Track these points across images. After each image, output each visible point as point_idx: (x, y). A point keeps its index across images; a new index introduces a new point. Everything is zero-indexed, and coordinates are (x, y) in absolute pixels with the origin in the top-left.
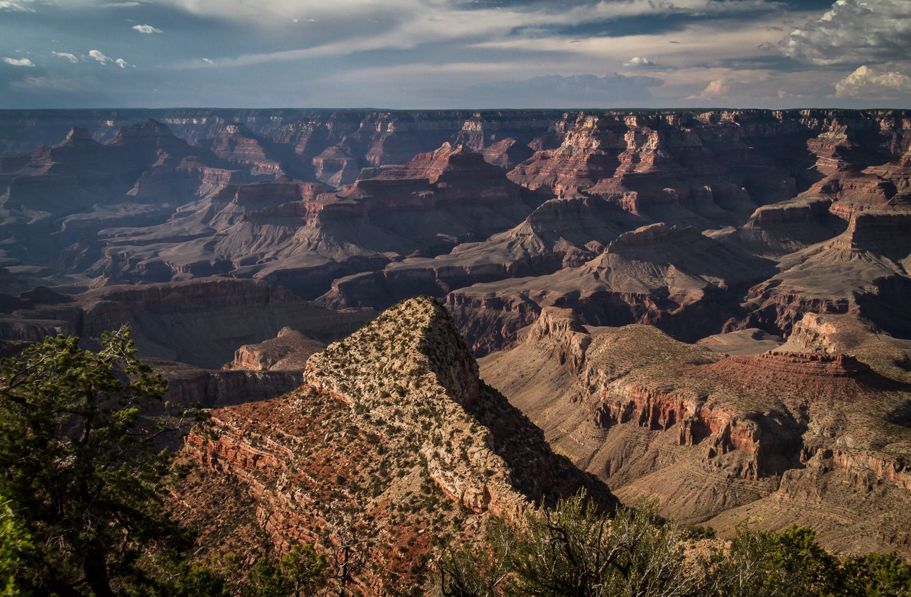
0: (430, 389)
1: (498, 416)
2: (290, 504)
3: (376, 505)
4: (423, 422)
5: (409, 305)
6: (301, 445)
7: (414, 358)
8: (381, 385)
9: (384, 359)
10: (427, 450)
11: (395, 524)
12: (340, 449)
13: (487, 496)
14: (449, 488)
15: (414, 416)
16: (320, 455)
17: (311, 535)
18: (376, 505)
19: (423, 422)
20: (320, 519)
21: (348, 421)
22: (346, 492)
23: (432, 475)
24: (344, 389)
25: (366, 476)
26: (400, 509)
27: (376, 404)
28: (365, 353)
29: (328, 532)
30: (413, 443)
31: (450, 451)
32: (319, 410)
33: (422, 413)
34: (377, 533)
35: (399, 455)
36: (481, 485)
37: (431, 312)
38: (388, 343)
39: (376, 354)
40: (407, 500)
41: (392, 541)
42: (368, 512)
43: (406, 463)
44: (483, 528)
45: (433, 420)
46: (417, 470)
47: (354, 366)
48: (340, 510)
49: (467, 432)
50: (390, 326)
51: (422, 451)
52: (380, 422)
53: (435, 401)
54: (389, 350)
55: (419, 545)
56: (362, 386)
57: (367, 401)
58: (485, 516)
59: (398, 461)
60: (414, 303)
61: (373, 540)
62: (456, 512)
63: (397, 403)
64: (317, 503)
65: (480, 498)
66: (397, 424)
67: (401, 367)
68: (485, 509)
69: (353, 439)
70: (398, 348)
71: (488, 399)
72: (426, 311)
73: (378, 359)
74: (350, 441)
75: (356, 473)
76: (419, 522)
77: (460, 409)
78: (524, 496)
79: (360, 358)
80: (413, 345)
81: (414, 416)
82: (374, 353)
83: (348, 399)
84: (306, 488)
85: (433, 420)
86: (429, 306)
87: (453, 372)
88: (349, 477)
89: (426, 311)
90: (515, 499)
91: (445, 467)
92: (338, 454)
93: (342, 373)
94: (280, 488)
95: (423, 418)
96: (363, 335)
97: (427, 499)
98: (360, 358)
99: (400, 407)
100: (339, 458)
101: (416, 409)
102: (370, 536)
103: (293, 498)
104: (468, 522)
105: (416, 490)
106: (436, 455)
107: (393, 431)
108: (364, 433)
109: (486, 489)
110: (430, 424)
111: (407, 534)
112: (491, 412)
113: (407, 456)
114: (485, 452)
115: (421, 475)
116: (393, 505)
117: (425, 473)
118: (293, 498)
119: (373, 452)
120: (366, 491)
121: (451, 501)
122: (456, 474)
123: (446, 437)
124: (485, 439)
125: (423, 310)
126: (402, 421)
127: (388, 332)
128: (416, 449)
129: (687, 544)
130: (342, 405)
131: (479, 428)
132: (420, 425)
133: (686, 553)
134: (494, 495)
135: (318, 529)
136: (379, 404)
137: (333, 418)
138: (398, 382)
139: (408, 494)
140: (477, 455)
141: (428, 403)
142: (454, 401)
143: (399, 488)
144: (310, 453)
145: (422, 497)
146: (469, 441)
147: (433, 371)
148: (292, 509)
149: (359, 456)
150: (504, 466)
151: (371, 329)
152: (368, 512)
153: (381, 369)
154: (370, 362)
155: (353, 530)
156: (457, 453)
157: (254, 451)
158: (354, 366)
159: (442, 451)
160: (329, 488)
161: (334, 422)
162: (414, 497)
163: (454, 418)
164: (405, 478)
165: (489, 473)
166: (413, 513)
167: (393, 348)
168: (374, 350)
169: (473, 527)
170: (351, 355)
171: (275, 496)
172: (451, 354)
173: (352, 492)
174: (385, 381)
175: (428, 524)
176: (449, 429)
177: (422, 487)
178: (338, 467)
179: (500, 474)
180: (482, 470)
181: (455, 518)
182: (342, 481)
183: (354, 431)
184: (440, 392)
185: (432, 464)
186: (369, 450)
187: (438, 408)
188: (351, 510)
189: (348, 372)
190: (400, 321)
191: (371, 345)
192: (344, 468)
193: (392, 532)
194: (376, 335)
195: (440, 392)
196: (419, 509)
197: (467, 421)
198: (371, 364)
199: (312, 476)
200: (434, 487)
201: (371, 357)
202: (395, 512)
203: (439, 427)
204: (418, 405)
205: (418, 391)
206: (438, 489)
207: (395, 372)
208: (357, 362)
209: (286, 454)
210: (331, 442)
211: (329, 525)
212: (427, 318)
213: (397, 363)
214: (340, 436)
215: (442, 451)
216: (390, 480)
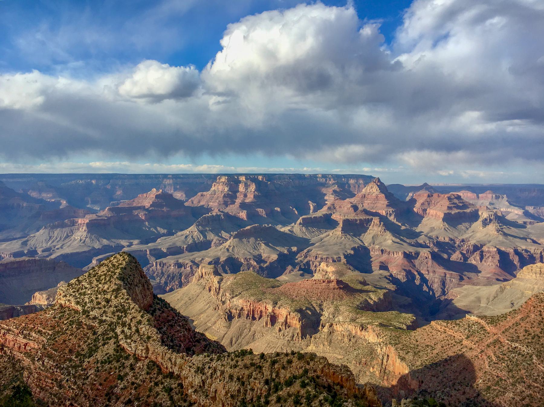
0: (122, 298)
1: (163, 312)
2: (41, 367)
3: (89, 362)
4: (118, 316)
5: (115, 257)
6: (51, 335)
9: (100, 286)
10: (118, 330)
11: (98, 371)
12: (72, 334)
13: (147, 349)
14: (129, 348)
15: (113, 313)
16: (60, 339)
17: (52, 383)
18: (89, 362)
19: (118, 316)
20: (57, 372)
21: (78, 319)
22: (73, 357)
23: (120, 343)
24: (78, 303)
25: (85, 347)
26: (102, 362)
27: (93, 309)
28: (90, 283)
29: (61, 381)
30: (112, 327)
31: (130, 328)
32: (63, 315)
33: (117, 311)
34: (88, 378)
35: (104, 334)
36: (145, 344)
37: (127, 260)
39: (97, 284)
40: (106, 358)
41: (95, 381)
42: (84, 367)
44: (145, 367)
46: (113, 341)
47: (84, 290)
48: (69, 367)
49: (139, 318)
52: (95, 318)
53: (125, 305)
54: (103, 281)
55: (110, 381)
56: (87, 301)
57: (88, 308)
58: (147, 361)
59: (103, 338)
60: (118, 256)
61: (87, 381)
62: (132, 361)
63: (105, 307)
64: (57, 365)
65: (144, 351)
66: (104, 318)
67: (108, 289)
68: (146, 357)
69: (79, 328)
71: (158, 304)
72: (124, 260)
73: (97, 286)
74: (77, 330)
75: (79, 346)
76: (111, 368)
77: (137, 306)
78: (166, 348)
79: (88, 286)
80: (115, 277)
81: (113, 313)
82: (95, 282)
83: (80, 308)
84: (50, 357)
87: (138, 290)
88: (75, 349)
89: (124, 260)
90: (161, 349)
91: (126, 337)
92: (71, 337)
93: (77, 295)
94: (36, 359)
95: (118, 313)
96: (90, 274)
97: (117, 355)
98: (88, 286)
99: (106, 309)
100: (71, 339)
101: (115, 309)
102: (84, 379)
103: (43, 363)
104: (138, 365)
105: (111, 352)
106: (123, 332)
107: (101, 322)
108: (86, 324)
109: (147, 346)
110: (122, 316)
111: (104, 375)
112: (159, 310)
113: (108, 334)
114: (147, 327)
115: (114, 343)
116: (98, 361)
118: (43, 363)
119: (90, 335)
120: (84, 355)
121: (129, 355)
122: (132, 340)
123: (128, 321)
124: (148, 320)
125: (122, 259)
126: (107, 317)
128: (113, 330)
129: (240, 359)
130: (76, 312)
131: (145, 315)
132: (116, 317)
133: (239, 363)
134: (151, 349)
135: (57, 379)
136: (95, 308)
137: (70, 319)
138: (106, 296)
139: (106, 354)
140: (144, 329)
141: (121, 305)
143: (102, 351)
144: (55, 339)
145: (114, 355)
146: (140, 322)
147: (125, 289)
148: (42, 370)
149: (82, 337)
150: (157, 333)
151: (95, 271)
152: (84, 367)
153: (97, 291)
154: (93, 288)
155: (75, 377)
156: (134, 329)
157: (25, 341)
158: (84, 290)
159: (126, 329)
160: (64, 356)
161: (71, 321)
162: (110, 356)
163: (134, 312)
165: (149, 338)
166: (109, 364)
167: (105, 279)
168: (96, 281)
169: (140, 368)
170: (82, 285)
171: (34, 364)
172: (136, 280)
173: (76, 357)
174: (99, 296)
175: (116, 369)
176: (130, 317)
177: (114, 350)
178: (70, 345)
179: (155, 338)
180: (146, 336)
181: (131, 364)
182: (71, 351)
183: (80, 324)
184: (128, 299)
185: (120, 337)
186: (88, 333)
187: (126, 307)
188: (75, 367)
189: (80, 294)
190: (110, 265)
192: (73, 344)
193: (96, 376)
194: (97, 273)
195: (128, 299)
196: (112, 361)
197: (140, 312)
199: (56, 351)
200: (121, 349)
201: (93, 285)
202: (99, 365)
203: (125, 317)
204: (116, 307)
206: (123, 349)
207: (105, 291)
208: (86, 288)
209: (43, 341)
210: (67, 332)
211: (63, 376)
213: (106, 286)
214: (72, 327)
215: (126, 329)
216: (98, 348)
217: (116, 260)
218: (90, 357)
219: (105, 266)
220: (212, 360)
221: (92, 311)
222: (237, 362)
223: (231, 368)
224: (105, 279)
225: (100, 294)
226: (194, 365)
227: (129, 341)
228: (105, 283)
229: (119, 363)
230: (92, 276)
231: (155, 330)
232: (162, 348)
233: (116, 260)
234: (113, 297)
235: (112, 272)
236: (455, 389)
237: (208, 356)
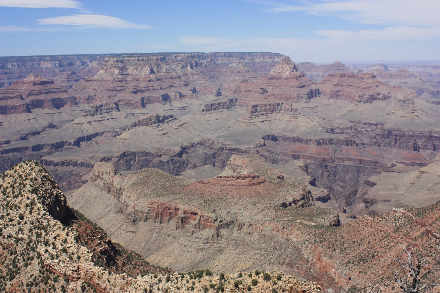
8: (8, 214)
9: (9, 199)
10: (41, 249)
31: (54, 248)
33: (35, 227)
40: (31, 280)
43: (29, 259)
45: (42, 231)
46: (36, 261)
51: (38, 250)
52: (10, 236)
59: (23, 258)
60: (24, 165)
66: (20, 236)
67: (20, 203)
70: (17, 192)
77: (59, 223)
78: (102, 268)
85: (42, 231)
89: (32, 169)
95: (36, 230)
104: (70, 287)
105: (36, 273)
106: (47, 251)
107: (18, 240)
117: (41, 262)
125: (30, 168)
127: (9, 183)
128: (34, 250)
129: (197, 280)
132: (35, 235)
133: (196, 285)
139: (31, 276)
141: (39, 222)
142: (55, 218)
150: (88, 252)
153: (7, 205)
159: (50, 249)
162: (36, 277)
164: (29, 267)
166: (36, 286)
167: (13, 192)
174: (10, 212)
177: (40, 271)
184: (45, 215)
190: (17, 176)
213: (17, 201)
215: (50, 249)
217: (22, 170)
218: (12, 278)
219: (11, 176)
220: (160, 281)
221: (5, 228)
222: (194, 283)
223: (188, 290)
224: (13, 192)
225: (11, 209)
228: (17, 197)
229: (48, 285)
231: (86, 248)
232: (96, 268)
233: (22, 170)
236: (385, 285)
237: (155, 277)
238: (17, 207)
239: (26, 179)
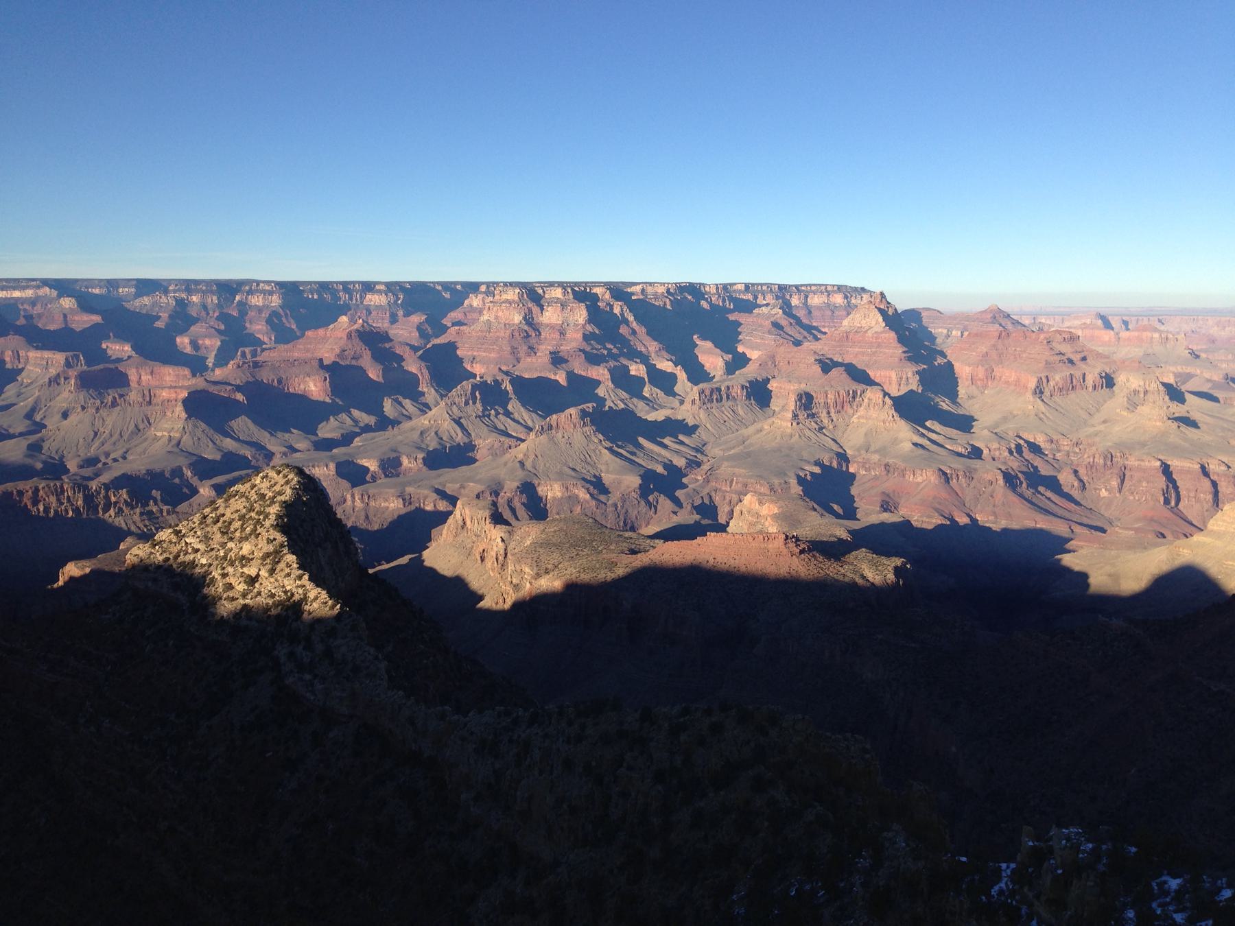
7: (269, 537)
9: (230, 545)
10: (282, 652)
28: (206, 539)
37: (294, 482)
38: (237, 524)
50: (238, 504)
54: (238, 534)
60: (272, 474)
72: (287, 483)
73: (223, 545)
78: (401, 693)
79: (202, 547)
80: (267, 523)
82: (218, 537)
86: (291, 476)
89: (287, 483)
98: (202, 547)
106: (291, 655)
125: (282, 481)
127: (237, 511)
138: (245, 570)
141: (286, 592)
142: (318, 586)
150: (376, 658)
153: (225, 558)
158: (191, 557)
167: (243, 529)
168: (219, 535)
174: (230, 570)
190: (254, 497)
191: (215, 528)
195: (300, 577)
198: (213, 553)
205: (272, 580)
207: (243, 557)
212: (289, 491)
213: (246, 548)
217: (266, 484)
226: (472, 733)
227: (308, 677)
228: (241, 540)
230: (209, 521)
231: (372, 650)
233: (266, 484)
234: (264, 573)
235: (259, 513)
238: (245, 560)
239: (273, 503)
